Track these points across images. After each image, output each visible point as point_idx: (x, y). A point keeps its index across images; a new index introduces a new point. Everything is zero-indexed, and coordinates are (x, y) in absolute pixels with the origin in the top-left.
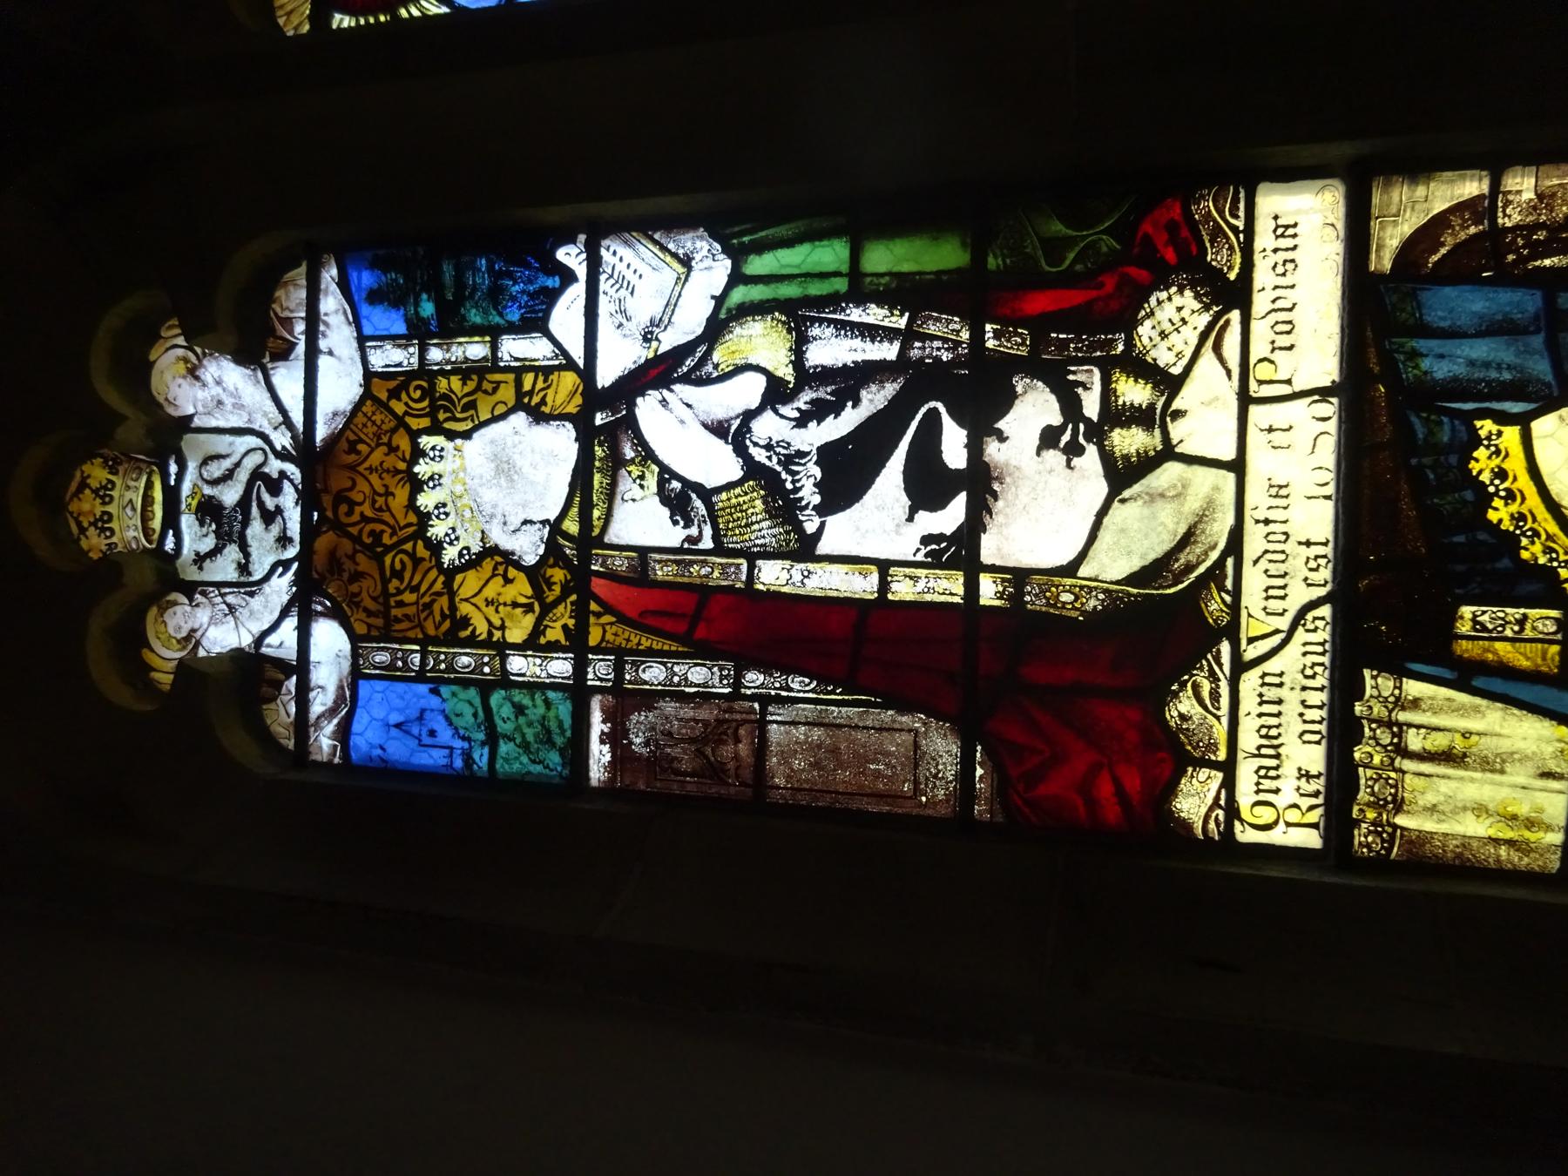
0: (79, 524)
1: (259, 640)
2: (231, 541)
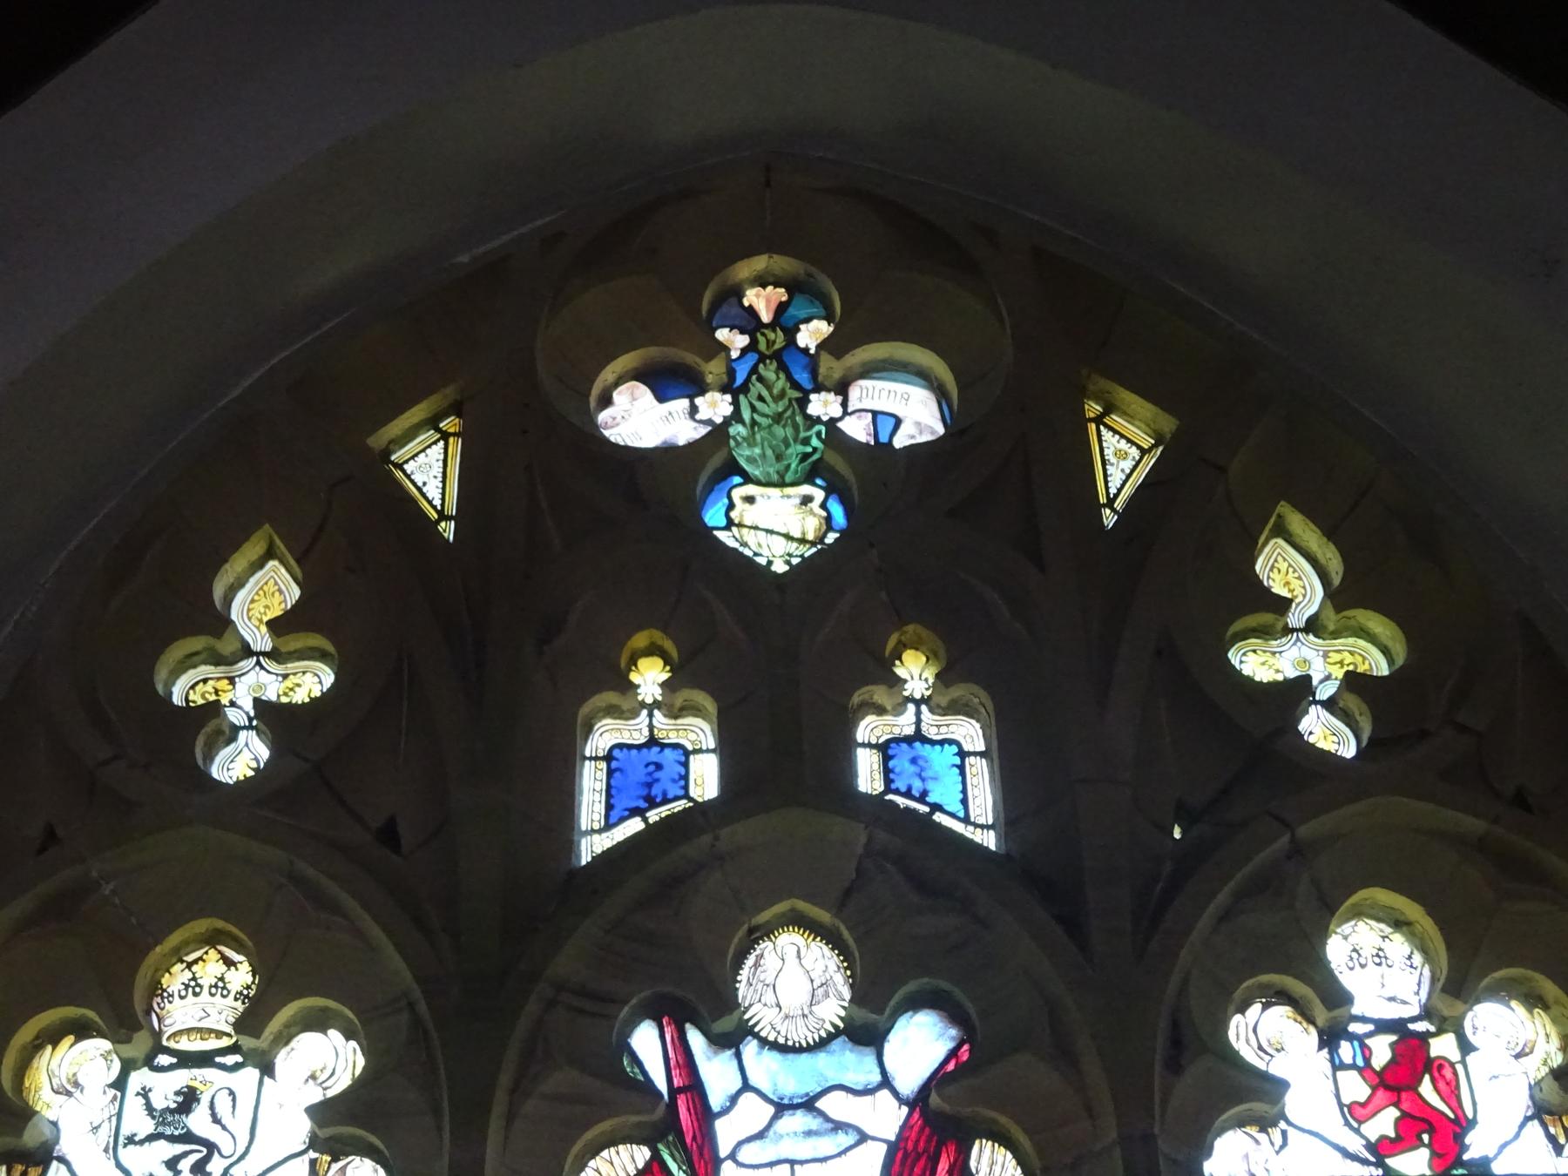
0: (196, 962)
1: (62, 1160)
2: (157, 1125)
